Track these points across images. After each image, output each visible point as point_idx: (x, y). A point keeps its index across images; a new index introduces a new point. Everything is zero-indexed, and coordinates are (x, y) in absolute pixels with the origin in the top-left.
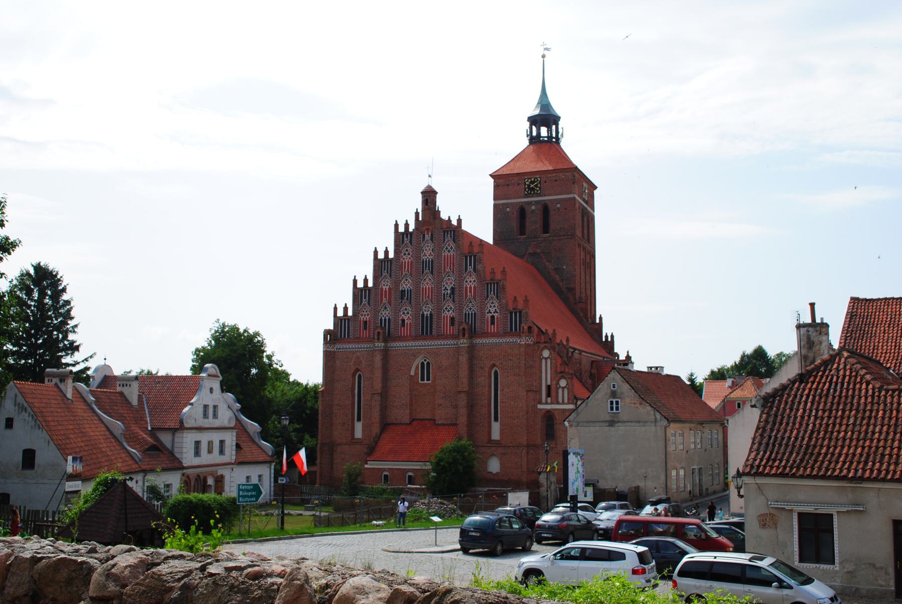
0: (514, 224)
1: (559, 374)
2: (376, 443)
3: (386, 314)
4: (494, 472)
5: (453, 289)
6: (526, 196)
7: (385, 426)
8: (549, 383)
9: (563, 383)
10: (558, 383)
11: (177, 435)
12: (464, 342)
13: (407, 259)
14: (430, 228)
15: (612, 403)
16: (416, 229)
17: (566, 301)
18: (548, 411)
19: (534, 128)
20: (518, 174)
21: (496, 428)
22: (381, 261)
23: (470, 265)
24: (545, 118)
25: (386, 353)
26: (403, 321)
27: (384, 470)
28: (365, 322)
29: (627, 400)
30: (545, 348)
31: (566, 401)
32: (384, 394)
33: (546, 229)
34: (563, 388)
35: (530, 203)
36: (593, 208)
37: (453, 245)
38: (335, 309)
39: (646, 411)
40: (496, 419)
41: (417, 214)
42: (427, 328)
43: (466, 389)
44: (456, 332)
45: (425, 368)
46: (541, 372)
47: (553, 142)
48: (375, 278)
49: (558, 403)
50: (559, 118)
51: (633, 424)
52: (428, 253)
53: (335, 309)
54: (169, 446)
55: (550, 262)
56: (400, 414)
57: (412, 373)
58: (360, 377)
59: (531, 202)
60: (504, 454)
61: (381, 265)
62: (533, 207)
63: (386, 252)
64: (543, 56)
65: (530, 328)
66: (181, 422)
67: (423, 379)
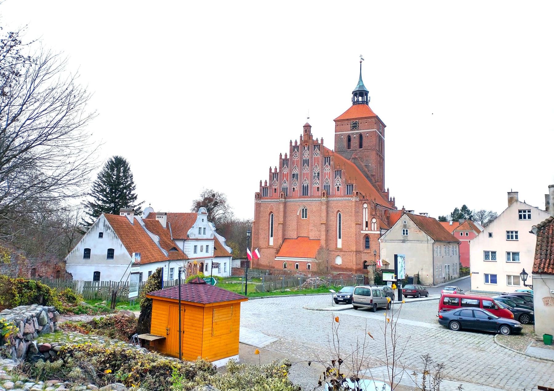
0: (345, 144)
1: (372, 216)
3: (286, 185)
5: (318, 173)
6: (351, 130)
7: (284, 240)
11: (186, 242)
12: (324, 199)
16: (301, 144)
17: (370, 181)
18: (367, 234)
21: (340, 242)
26: (294, 189)
28: (275, 189)
29: (412, 230)
30: (365, 203)
31: (376, 229)
32: (284, 224)
33: (361, 146)
35: (353, 134)
36: (384, 136)
37: (318, 151)
38: (261, 182)
39: (422, 235)
40: (340, 238)
41: (301, 136)
44: (320, 194)
48: (280, 168)
49: (371, 230)
52: (306, 156)
53: (261, 182)
54: (182, 248)
56: (292, 234)
58: (272, 215)
63: (286, 155)
66: (188, 236)
67: (303, 217)
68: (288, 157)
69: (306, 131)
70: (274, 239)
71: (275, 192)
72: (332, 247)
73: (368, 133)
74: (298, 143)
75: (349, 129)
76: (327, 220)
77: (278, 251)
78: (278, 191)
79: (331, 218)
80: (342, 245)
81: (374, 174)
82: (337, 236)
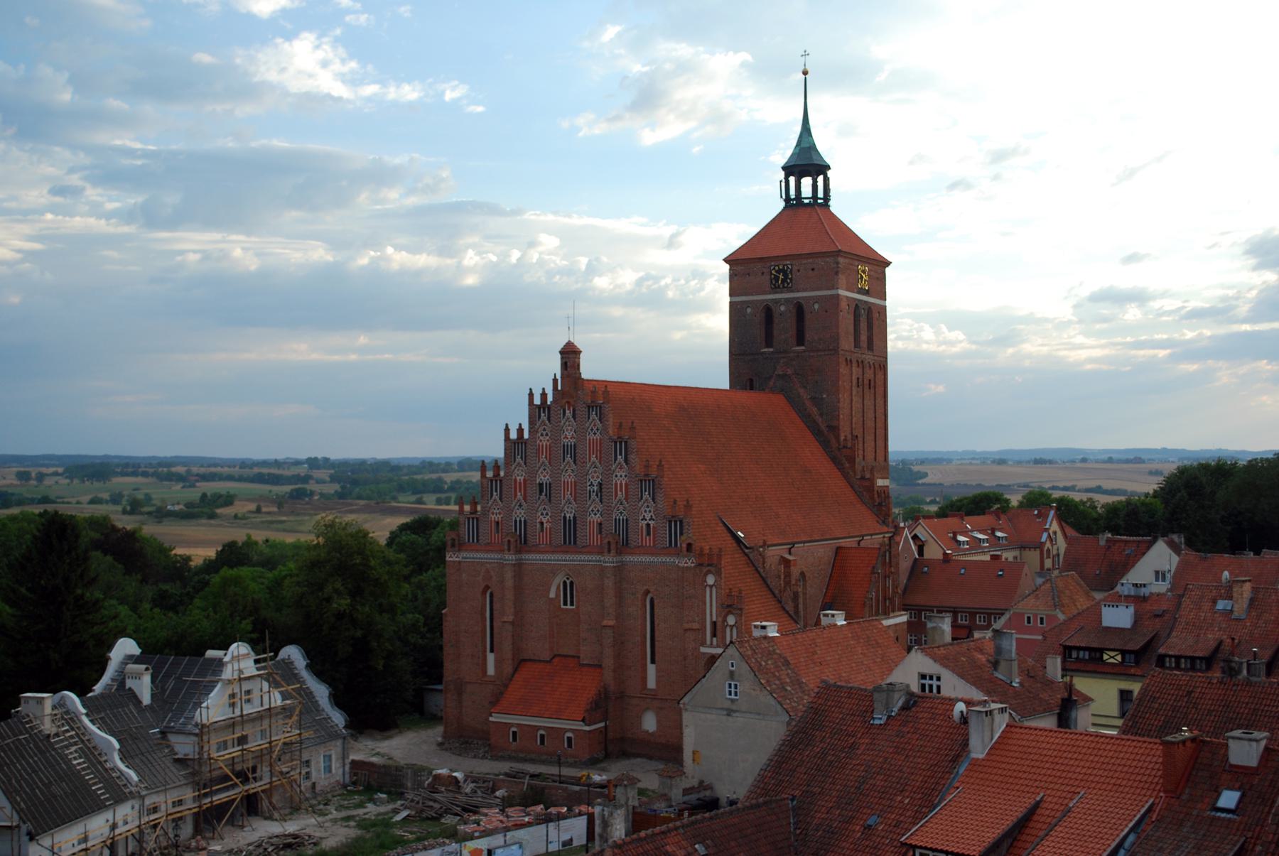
2: (506, 686)
3: (520, 514)
5: (600, 485)
7: (520, 663)
9: (731, 620)
10: (725, 620)
12: (609, 560)
13: (544, 441)
14: (571, 401)
17: (825, 444)
19: (792, 180)
20: (761, 259)
21: (651, 670)
22: (514, 442)
25: (519, 566)
26: (542, 523)
30: (709, 572)
33: (800, 340)
34: (732, 627)
35: (777, 302)
40: (653, 662)
42: (570, 534)
43: (611, 623)
45: (569, 589)
47: (821, 204)
50: (828, 167)
57: (552, 595)
61: (515, 446)
62: (783, 308)
64: (805, 73)
65: (689, 545)
67: (565, 604)
69: (565, 366)
70: (496, 661)
74: (550, 399)
80: (658, 682)
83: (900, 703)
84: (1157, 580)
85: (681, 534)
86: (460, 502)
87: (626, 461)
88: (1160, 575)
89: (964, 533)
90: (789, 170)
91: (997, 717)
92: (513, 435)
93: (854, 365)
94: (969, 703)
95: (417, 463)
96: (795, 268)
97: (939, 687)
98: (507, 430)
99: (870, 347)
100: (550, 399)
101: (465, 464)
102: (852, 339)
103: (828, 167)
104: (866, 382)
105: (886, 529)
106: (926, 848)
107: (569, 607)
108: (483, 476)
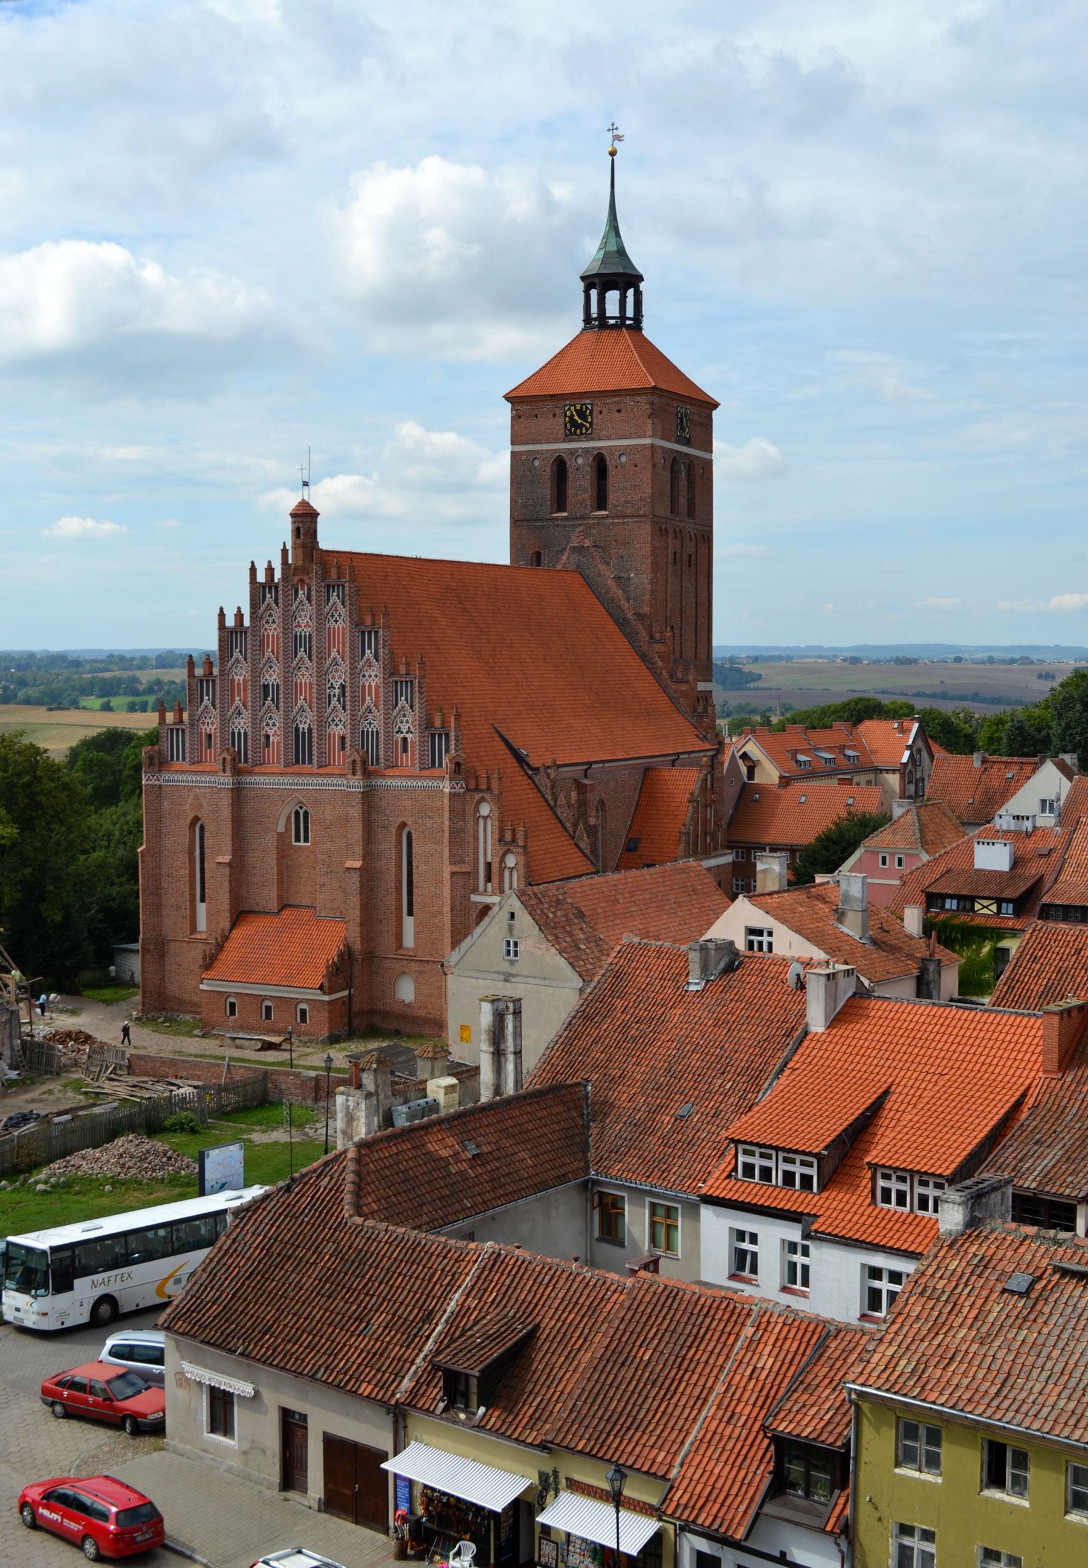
0: (546, 491)
1: (506, 843)
2: (220, 947)
4: (407, 1001)
5: (343, 687)
8: (489, 860)
10: (502, 860)
14: (306, 578)
15: (508, 943)
19: (594, 293)
20: (553, 397)
21: (409, 923)
22: (231, 632)
23: (370, 648)
24: (615, 276)
26: (267, 737)
27: (229, 995)
28: (210, 736)
30: (482, 800)
35: (573, 452)
43: (358, 864)
45: (301, 821)
46: (476, 839)
50: (640, 278)
51: (536, 981)
55: (608, 564)
58: (202, 829)
59: (576, 450)
60: (420, 972)
64: (613, 154)
67: (298, 839)
68: (247, 622)
69: (297, 532)
70: (208, 912)
71: (210, 747)
72: (386, 942)
73: (623, 451)
74: (278, 575)
75: (561, 435)
76: (368, 856)
77: (209, 963)
78: (216, 741)
79: (382, 847)
81: (647, 610)
82: (399, 909)
83: (722, 965)
84: (1043, 811)
85: (447, 751)
86: (161, 708)
87: (376, 657)
88: (1045, 805)
89: (803, 752)
90: (590, 281)
91: (842, 981)
92: (230, 622)
93: (671, 535)
94: (808, 964)
95: (103, 656)
96: (597, 409)
97: (770, 945)
98: (222, 615)
99: (691, 513)
100: (278, 575)
101: (165, 660)
102: (668, 501)
103: (640, 278)
104: (685, 558)
105: (708, 746)
106: (751, 1143)
107: (302, 844)
108: (191, 674)
